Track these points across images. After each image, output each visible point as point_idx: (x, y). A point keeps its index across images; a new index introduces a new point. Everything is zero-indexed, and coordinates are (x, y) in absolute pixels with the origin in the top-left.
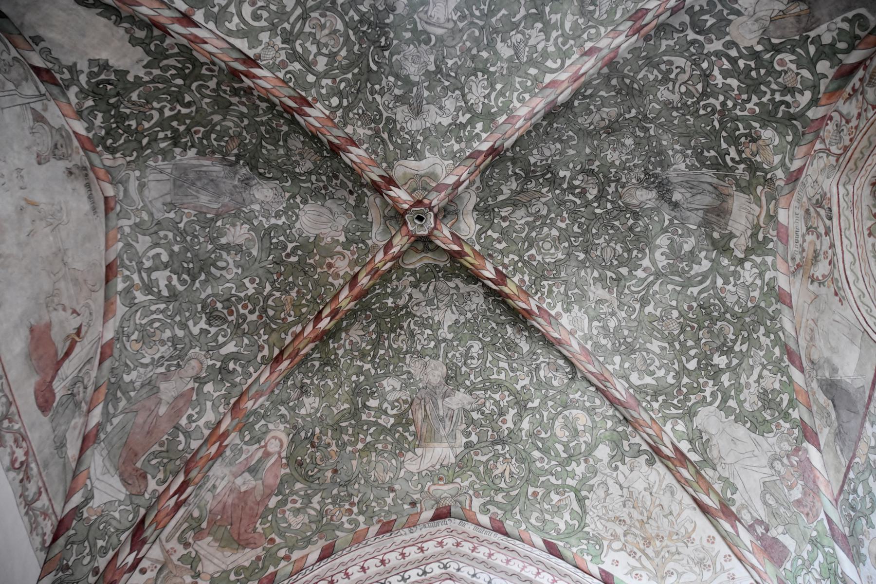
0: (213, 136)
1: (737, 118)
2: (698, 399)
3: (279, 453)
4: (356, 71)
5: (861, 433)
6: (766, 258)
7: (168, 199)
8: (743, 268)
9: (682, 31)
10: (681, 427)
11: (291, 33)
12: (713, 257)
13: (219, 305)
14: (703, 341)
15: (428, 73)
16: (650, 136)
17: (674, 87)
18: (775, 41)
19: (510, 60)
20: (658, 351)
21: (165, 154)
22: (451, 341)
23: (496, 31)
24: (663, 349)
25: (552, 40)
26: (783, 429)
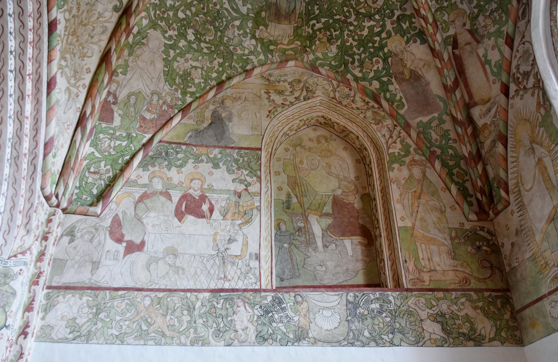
1: (342, 31)
2: (164, 27)
5: (210, 147)
6: (262, 54)
8: (251, 39)
9: (401, 8)
10: (145, 22)
12: (250, 15)
14: (198, 19)
18: (390, 59)
26: (176, 93)
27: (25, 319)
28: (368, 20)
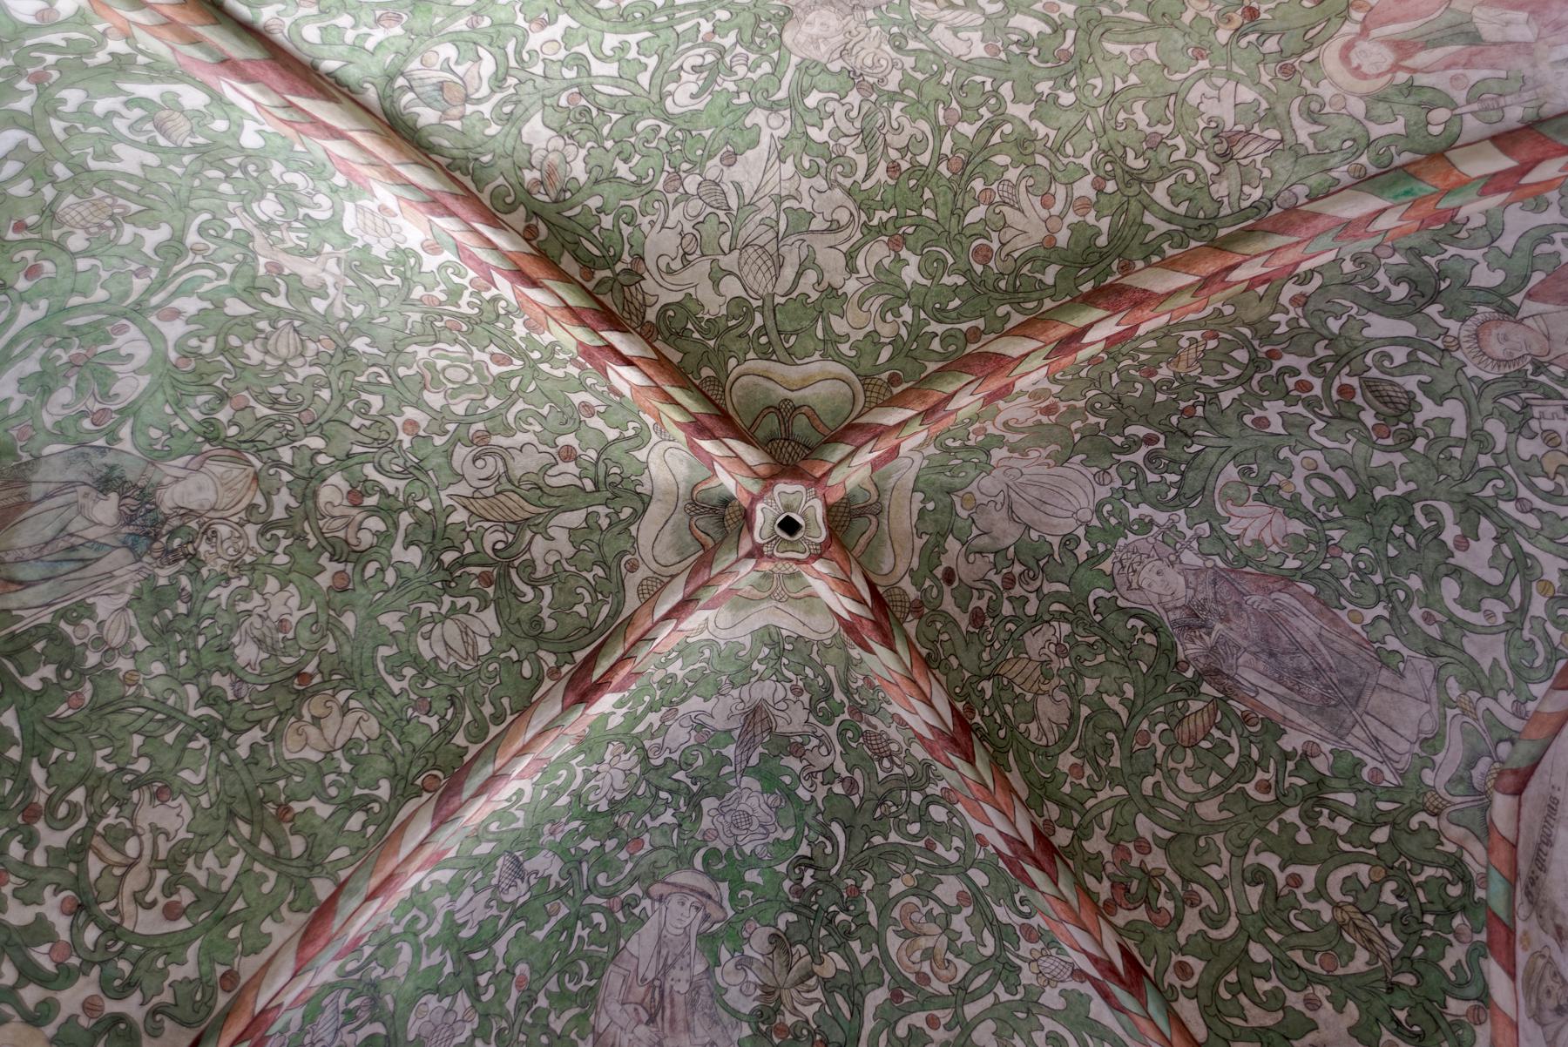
0: (1231, 761)
3: (1364, 32)
4: (878, 840)
7: (1385, 676)
9: (154, 1012)
11: (996, 977)
13: (1369, 418)
15: (719, 791)
16: (193, 680)
17: (155, 844)
19: (531, 852)
20: (120, 149)
21: (1351, 775)
22: (754, 104)
23: (560, 892)
24: (108, 155)
25: (440, 918)
28: (68, 906)
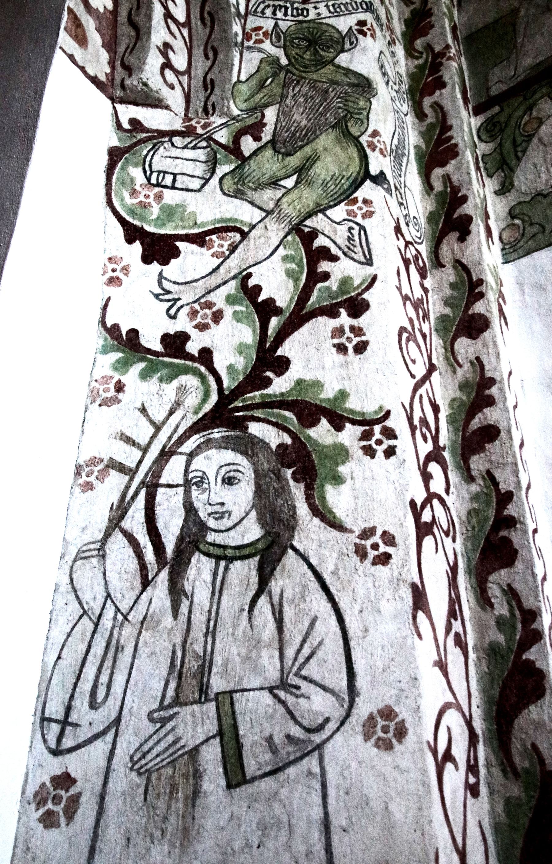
27: (438, 186)
